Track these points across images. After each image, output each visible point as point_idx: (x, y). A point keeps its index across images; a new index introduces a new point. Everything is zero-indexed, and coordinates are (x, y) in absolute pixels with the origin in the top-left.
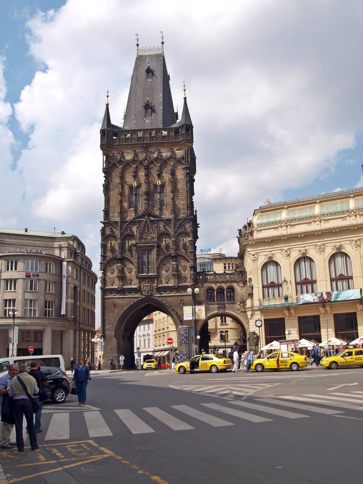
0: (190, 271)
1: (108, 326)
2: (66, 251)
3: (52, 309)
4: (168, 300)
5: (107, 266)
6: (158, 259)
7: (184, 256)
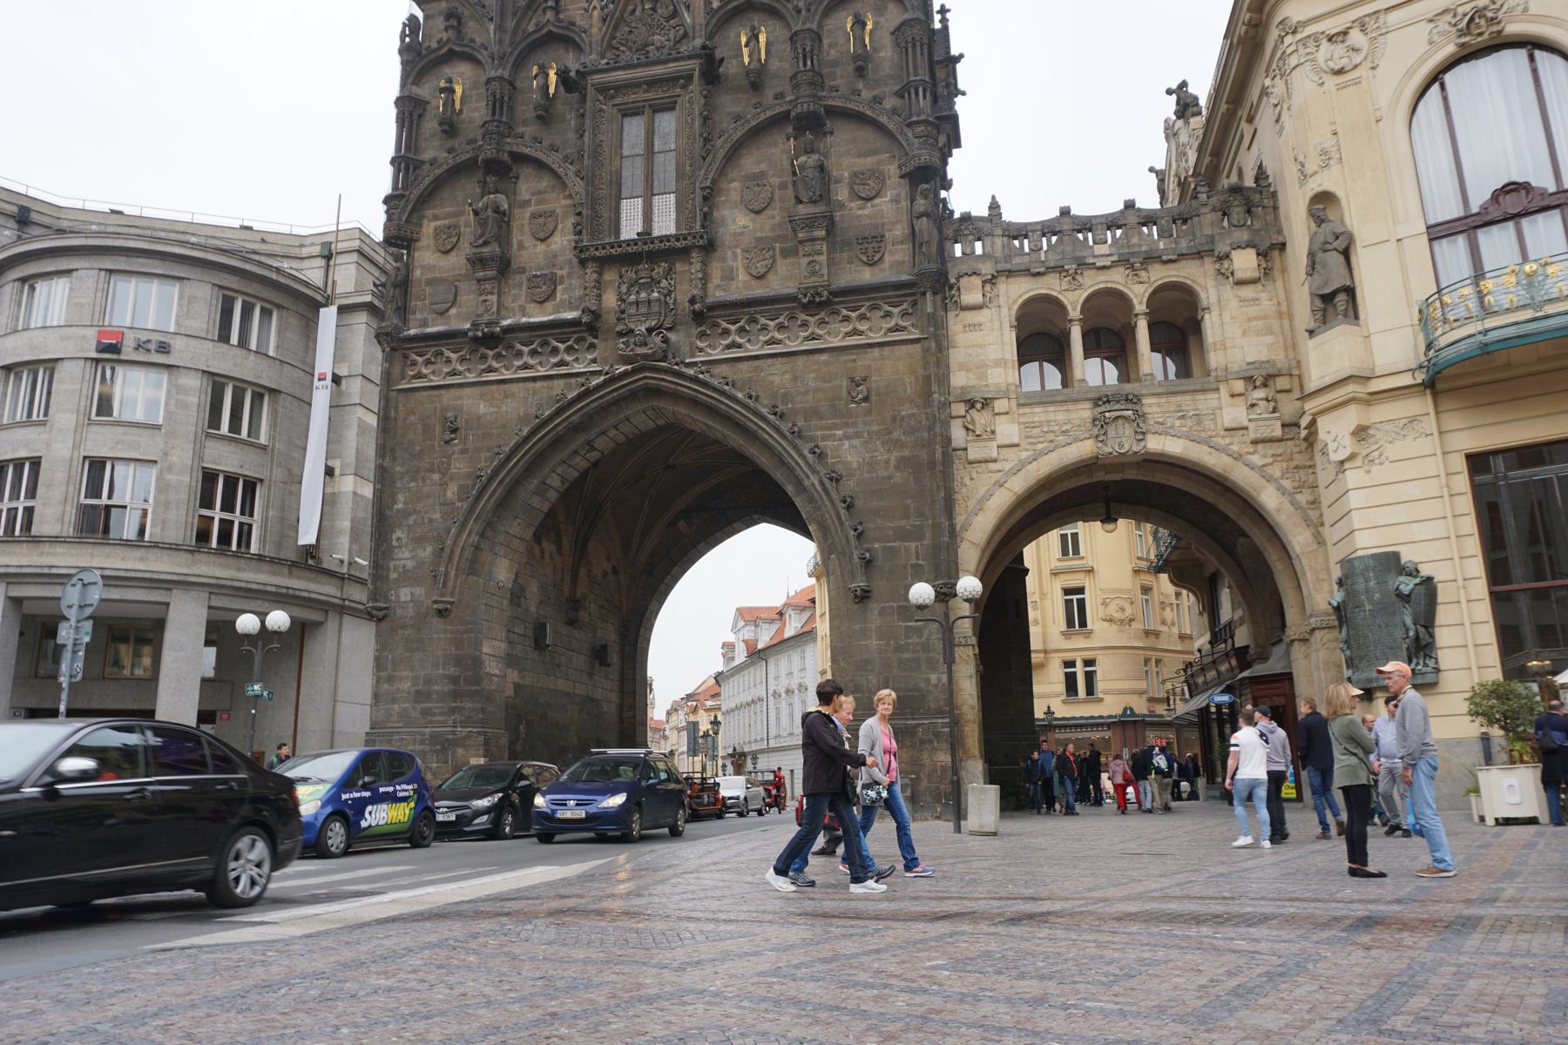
0: (904, 204)
1: (407, 554)
2: (352, 269)
3: (251, 515)
4: (772, 383)
5: (422, 217)
6: (707, 140)
7: (869, 113)
